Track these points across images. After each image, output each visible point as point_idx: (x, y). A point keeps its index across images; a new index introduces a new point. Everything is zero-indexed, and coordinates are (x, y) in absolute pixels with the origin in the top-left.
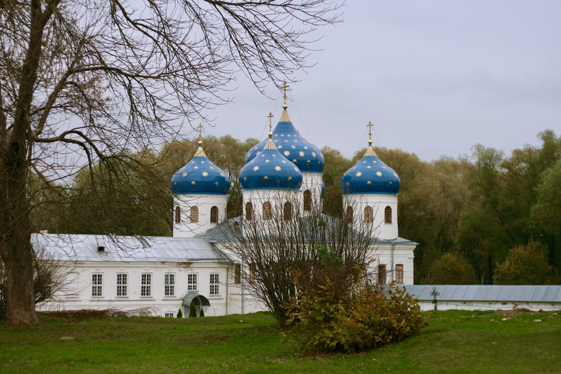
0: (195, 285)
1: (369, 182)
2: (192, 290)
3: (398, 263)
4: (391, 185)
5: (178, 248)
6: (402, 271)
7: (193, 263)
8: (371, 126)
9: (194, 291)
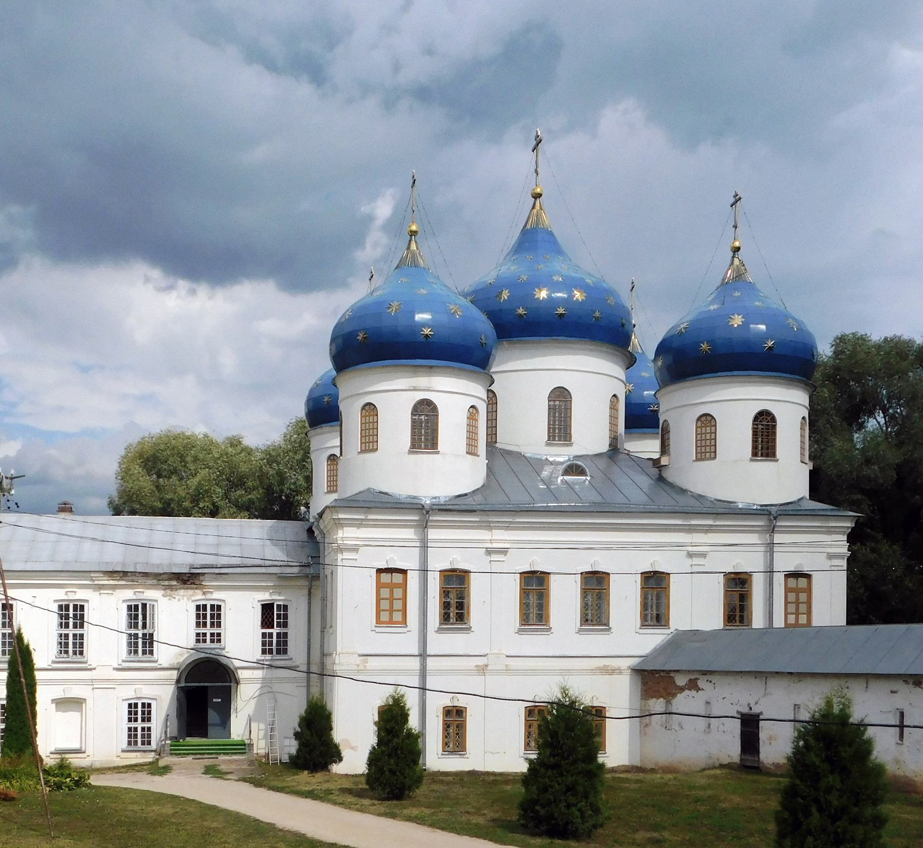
6: (809, 590)
7: (204, 574)
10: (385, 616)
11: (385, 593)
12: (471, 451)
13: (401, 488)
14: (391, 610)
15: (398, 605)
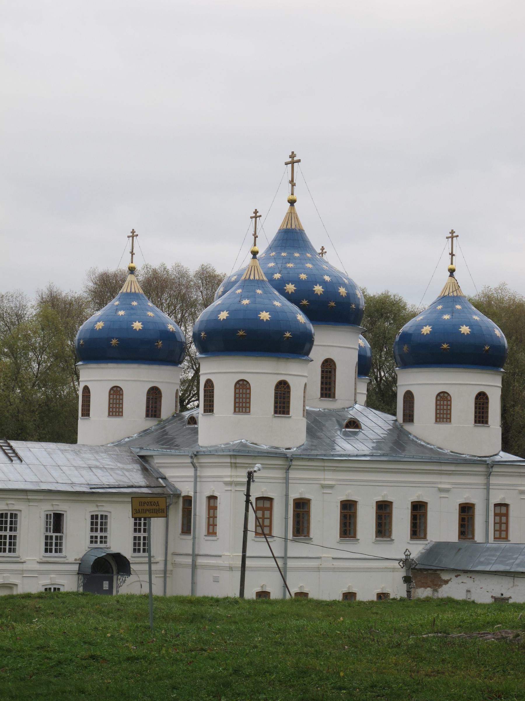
0: (103, 534)
1: (445, 346)
2: (99, 545)
3: (498, 501)
4: (487, 351)
5: (76, 465)
6: (507, 515)
8: (455, 239)
9: (103, 546)
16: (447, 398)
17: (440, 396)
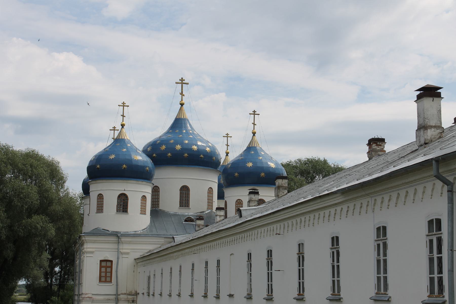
10: (103, 279)
11: (103, 269)
12: (143, 212)
13: (112, 228)
14: (106, 277)
15: (108, 274)
16: (241, 203)
17: (237, 202)
